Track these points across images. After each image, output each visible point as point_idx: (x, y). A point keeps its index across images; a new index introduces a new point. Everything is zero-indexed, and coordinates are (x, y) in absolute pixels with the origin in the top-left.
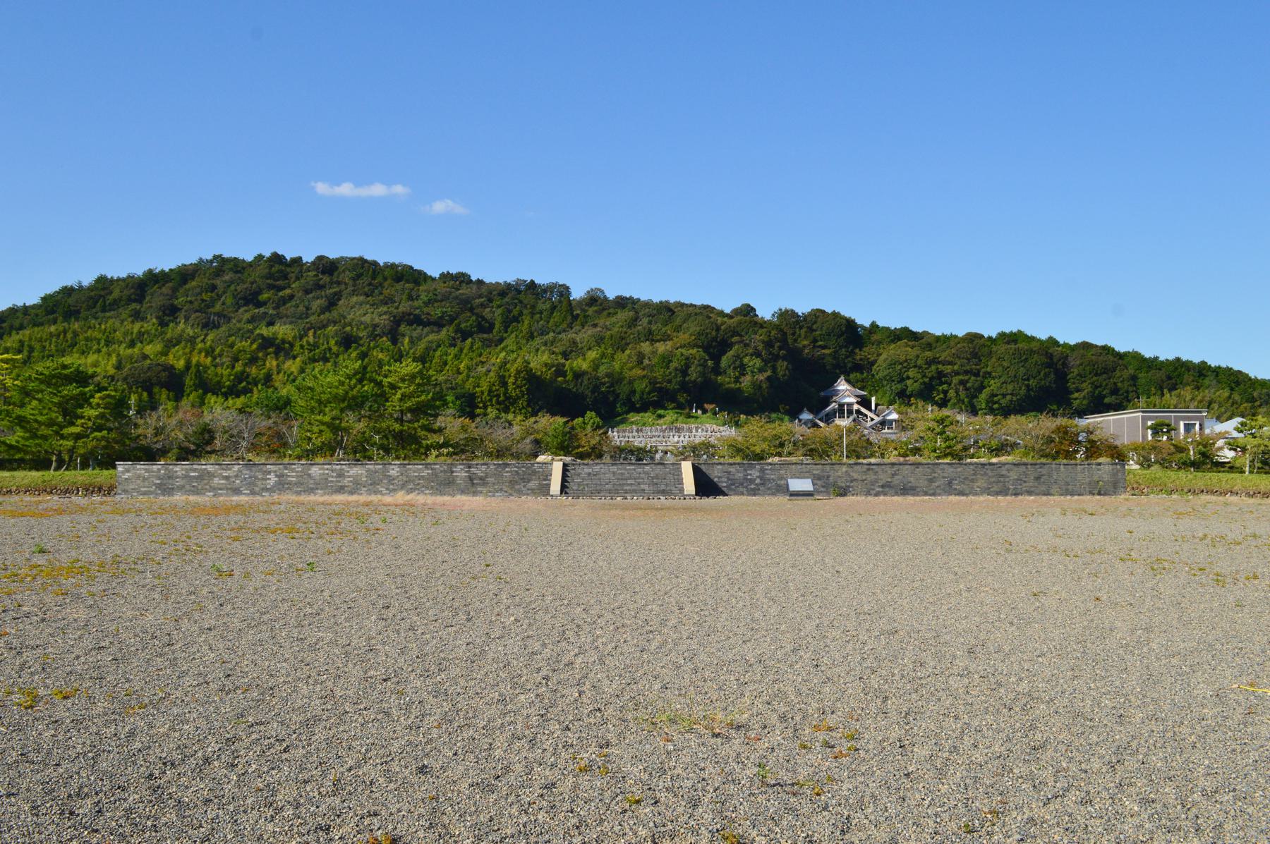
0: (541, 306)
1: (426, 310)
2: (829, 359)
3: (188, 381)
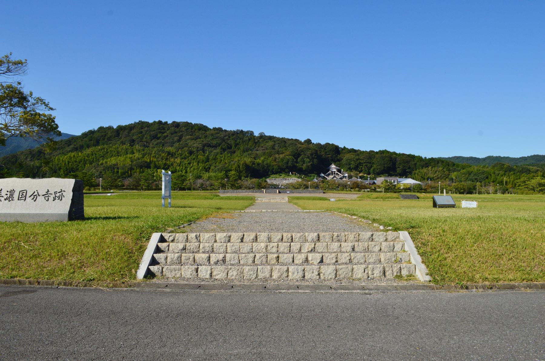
0: (245, 139)
1: (212, 141)
2: (330, 158)
3: (152, 166)
